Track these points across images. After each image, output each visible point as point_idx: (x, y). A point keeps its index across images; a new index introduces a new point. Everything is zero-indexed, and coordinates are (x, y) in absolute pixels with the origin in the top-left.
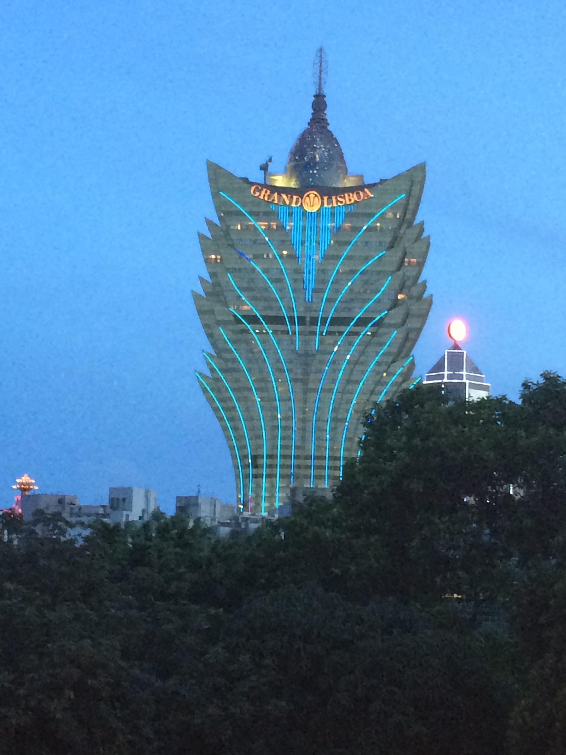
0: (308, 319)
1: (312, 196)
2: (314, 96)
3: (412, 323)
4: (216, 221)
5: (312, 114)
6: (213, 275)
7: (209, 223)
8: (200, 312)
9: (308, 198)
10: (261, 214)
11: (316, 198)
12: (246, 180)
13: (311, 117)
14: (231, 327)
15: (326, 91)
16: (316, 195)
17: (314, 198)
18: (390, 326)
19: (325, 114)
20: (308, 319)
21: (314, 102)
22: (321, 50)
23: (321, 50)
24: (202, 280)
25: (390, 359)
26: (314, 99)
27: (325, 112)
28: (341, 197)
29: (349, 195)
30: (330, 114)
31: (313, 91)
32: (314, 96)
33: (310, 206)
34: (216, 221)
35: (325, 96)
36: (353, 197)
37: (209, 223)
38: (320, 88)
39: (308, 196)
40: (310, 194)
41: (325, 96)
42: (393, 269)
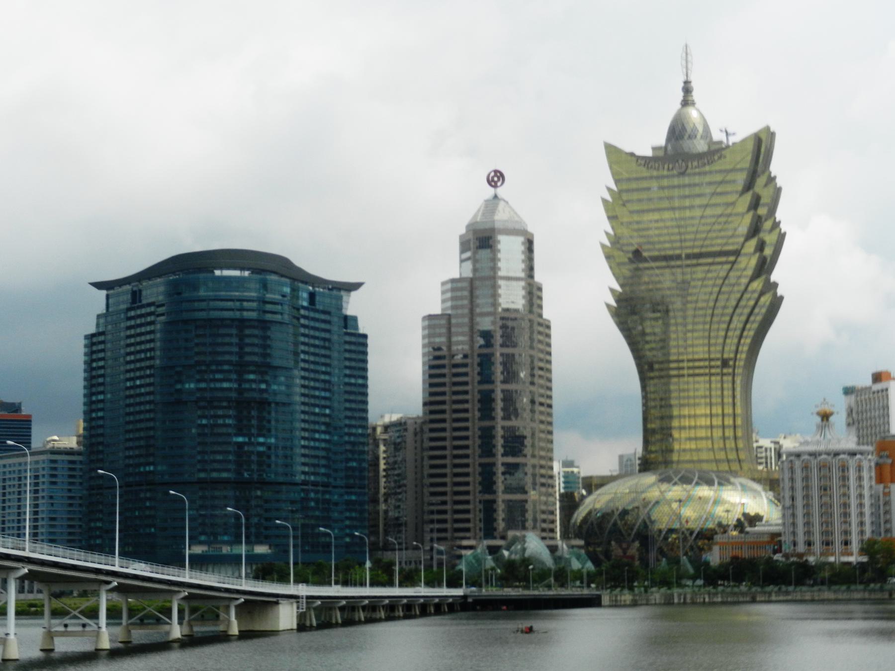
0: (683, 256)
1: (680, 162)
3: (768, 251)
4: (614, 187)
6: (613, 228)
7: (609, 189)
8: (608, 257)
12: (632, 154)
15: (692, 78)
16: (683, 160)
18: (746, 255)
20: (683, 256)
24: (607, 234)
30: (696, 95)
34: (614, 187)
35: (690, 82)
37: (609, 189)
39: (677, 161)
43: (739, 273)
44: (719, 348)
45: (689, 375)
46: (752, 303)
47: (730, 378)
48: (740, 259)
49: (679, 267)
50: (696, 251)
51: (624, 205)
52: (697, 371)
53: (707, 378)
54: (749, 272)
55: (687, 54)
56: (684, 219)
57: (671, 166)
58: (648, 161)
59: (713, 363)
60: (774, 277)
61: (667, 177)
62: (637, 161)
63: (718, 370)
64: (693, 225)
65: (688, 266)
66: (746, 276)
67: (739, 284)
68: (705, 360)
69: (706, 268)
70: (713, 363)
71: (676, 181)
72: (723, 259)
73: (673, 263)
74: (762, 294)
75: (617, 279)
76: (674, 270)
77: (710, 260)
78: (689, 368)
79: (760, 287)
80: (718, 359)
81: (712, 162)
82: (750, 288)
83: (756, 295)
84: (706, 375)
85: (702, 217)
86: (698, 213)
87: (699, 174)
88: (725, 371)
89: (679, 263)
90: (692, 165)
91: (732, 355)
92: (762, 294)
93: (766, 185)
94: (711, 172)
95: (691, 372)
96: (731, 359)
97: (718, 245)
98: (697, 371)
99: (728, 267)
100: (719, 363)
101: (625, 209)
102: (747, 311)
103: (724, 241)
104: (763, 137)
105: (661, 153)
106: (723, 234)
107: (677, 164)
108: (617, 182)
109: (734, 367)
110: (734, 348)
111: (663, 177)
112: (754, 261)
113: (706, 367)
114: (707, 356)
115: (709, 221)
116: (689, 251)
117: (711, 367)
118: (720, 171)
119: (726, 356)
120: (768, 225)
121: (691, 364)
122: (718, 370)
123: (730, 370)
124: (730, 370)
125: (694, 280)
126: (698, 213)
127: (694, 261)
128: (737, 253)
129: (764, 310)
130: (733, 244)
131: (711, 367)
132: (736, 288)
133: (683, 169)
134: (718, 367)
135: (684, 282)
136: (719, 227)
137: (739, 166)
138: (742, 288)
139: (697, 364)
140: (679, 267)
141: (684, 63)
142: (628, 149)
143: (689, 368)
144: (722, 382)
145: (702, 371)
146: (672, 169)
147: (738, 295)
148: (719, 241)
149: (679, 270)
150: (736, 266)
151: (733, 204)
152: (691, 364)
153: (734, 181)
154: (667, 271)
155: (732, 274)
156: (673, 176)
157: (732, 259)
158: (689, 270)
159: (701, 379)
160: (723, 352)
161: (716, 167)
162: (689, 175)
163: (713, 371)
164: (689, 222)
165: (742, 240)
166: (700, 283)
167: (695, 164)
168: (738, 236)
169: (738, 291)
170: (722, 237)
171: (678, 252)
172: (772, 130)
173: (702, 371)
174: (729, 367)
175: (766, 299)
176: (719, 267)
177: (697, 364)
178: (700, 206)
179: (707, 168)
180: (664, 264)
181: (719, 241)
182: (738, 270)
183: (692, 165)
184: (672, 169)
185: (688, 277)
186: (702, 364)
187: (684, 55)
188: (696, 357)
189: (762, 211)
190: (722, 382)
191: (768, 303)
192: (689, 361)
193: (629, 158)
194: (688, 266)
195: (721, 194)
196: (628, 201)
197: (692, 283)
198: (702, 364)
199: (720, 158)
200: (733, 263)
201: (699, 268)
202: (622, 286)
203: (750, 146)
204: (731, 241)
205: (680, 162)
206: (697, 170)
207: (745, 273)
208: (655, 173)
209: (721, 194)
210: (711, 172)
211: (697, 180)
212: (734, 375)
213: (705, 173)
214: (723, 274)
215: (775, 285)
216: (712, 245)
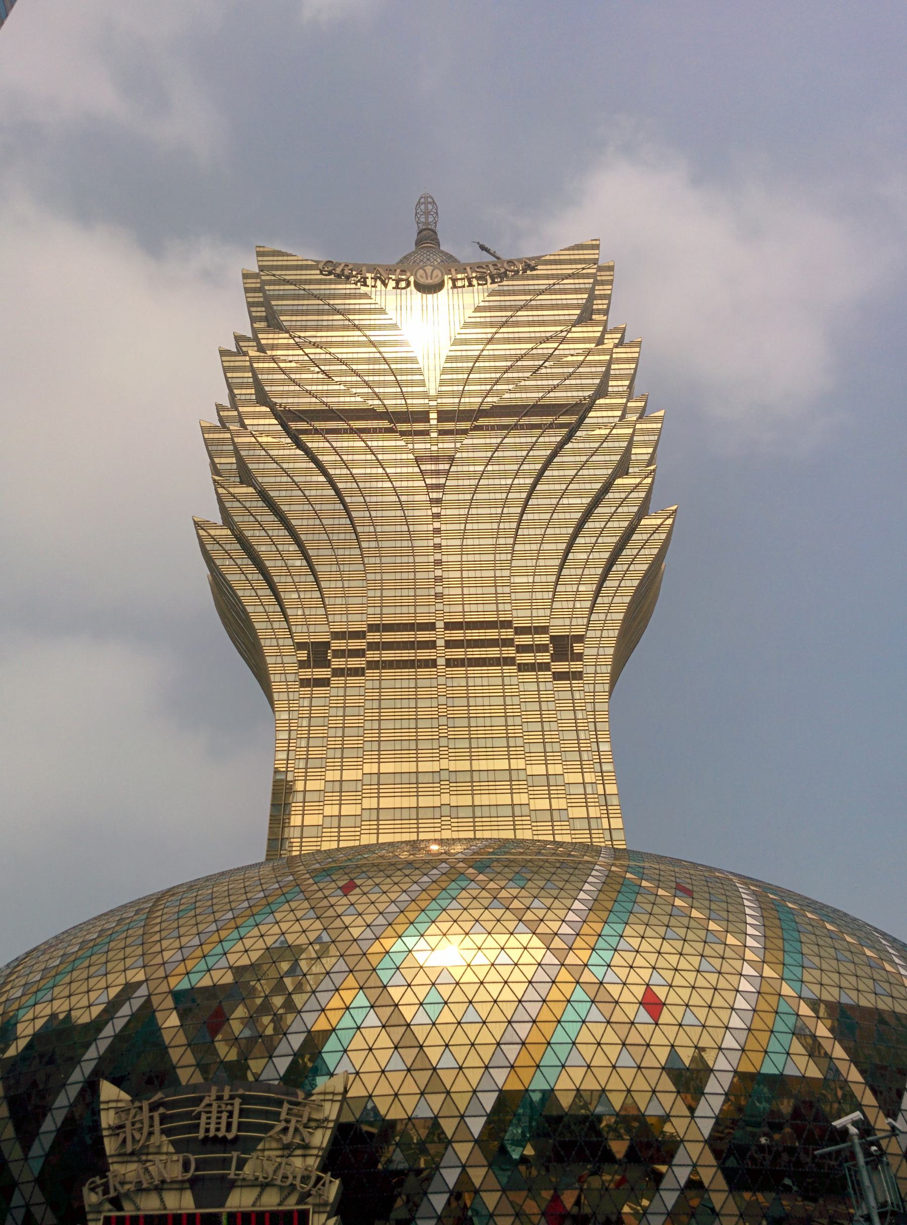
0: (433, 415)
20: (433, 415)
33: (427, 279)
59: (524, 640)
63: (544, 657)
72: (548, 420)
78: (449, 644)
88: (561, 667)
121: (458, 635)
122: (544, 657)
124: (576, 666)
128: (582, 410)
133: (437, 280)
143: (449, 644)
145: (493, 652)
152: (458, 635)
173: (493, 652)
200: (572, 430)
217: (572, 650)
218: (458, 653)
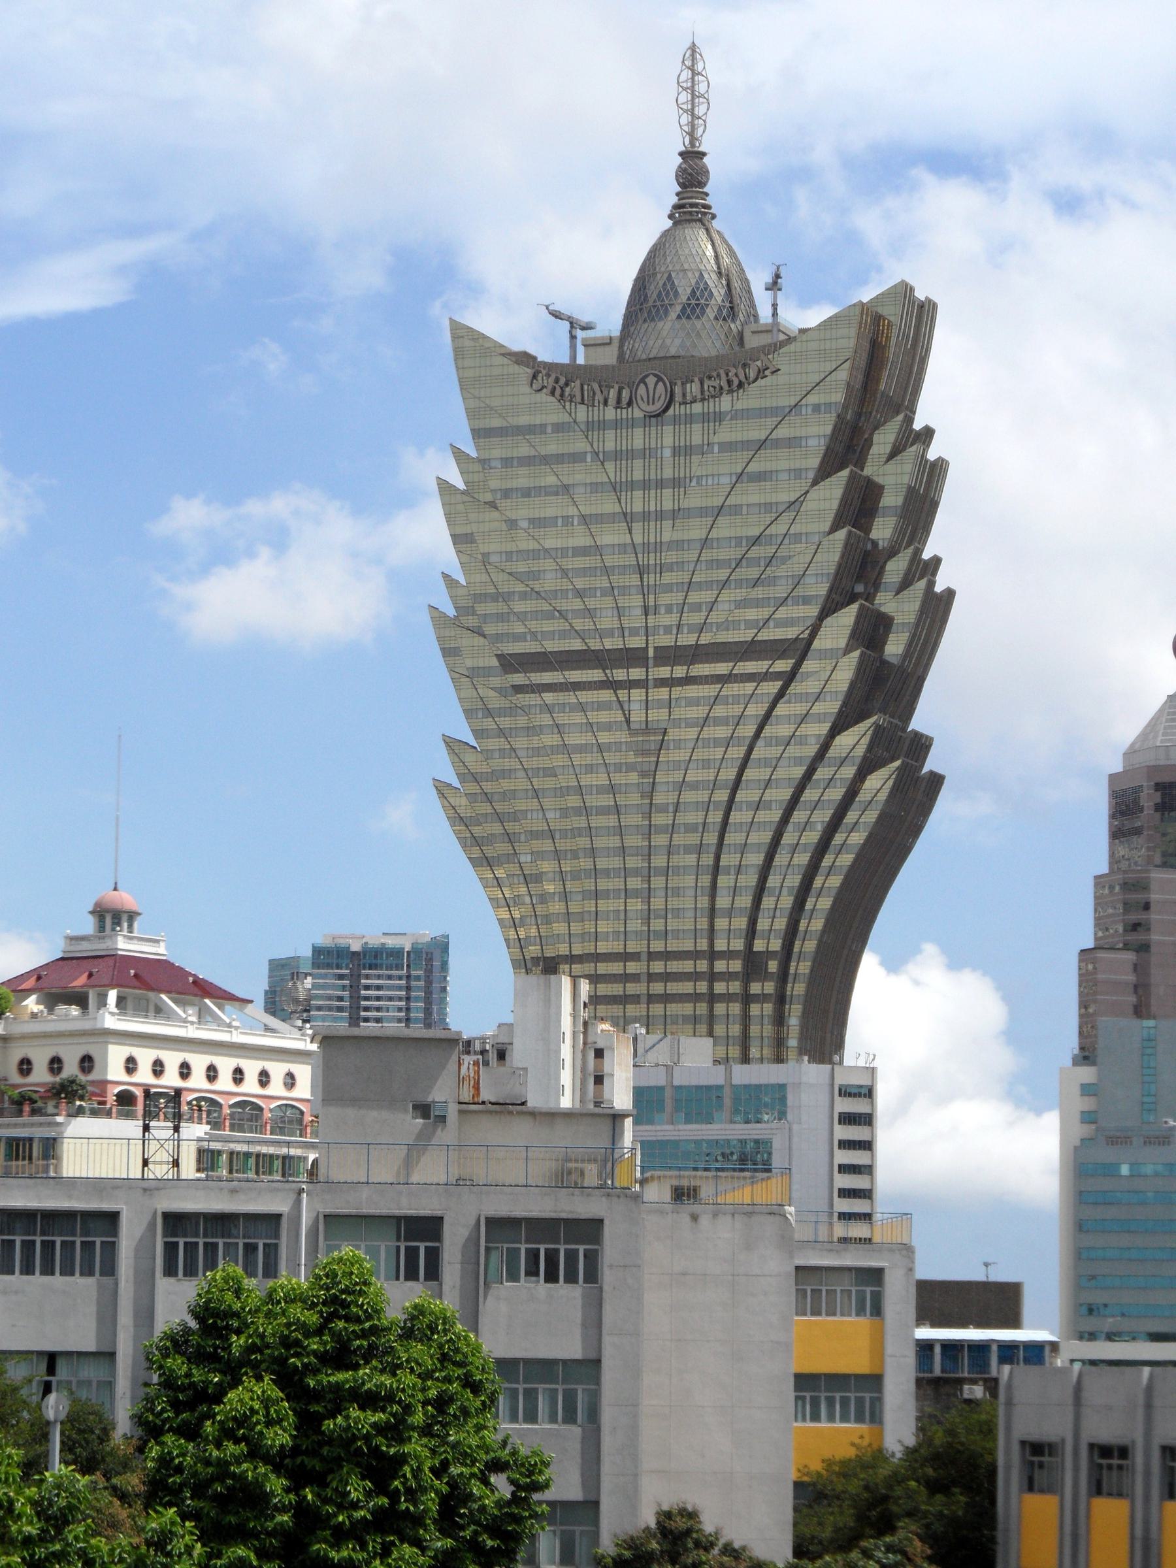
0: (651, 653)
1: (651, 381)
2: (681, 154)
3: (894, 647)
5: (677, 194)
8: (449, 652)
9: (642, 385)
10: (549, 429)
11: (661, 384)
12: (524, 358)
13: (674, 200)
14: (496, 681)
16: (660, 379)
17: (656, 384)
18: (824, 654)
19: (707, 194)
20: (651, 653)
21: (680, 167)
22: (693, 48)
23: (693, 48)
25: (825, 728)
26: (680, 160)
27: (705, 190)
28: (710, 378)
29: (727, 375)
30: (717, 192)
31: (679, 143)
32: (681, 154)
33: (648, 404)
35: (704, 154)
36: (736, 375)
38: (692, 134)
39: (643, 381)
40: (647, 376)
41: (704, 154)
42: (827, 529)
43: (800, 708)
44: (741, 923)
45: (651, 999)
46: (836, 794)
47: (768, 1008)
48: (808, 666)
49: (632, 684)
50: (688, 639)
51: (493, 505)
52: (674, 988)
53: (702, 1008)
54: (831, 707)
55: (695, 73)
56: (659, 547)
57: (625, 394)
58: (562, 380)
59: (720, 966)
60: (918, 723)
61: (616, 424)
62: (534, 377)
63: (735, 987)
64: (680, 565)
65: (662, 683)
66: (820, 718)
67: (803, 741)
68: (695, 955)
69: (711, 690)
70: (720, 966)
71: (638, 439)
73: (620, 674)
74: (866, 768)
75: (469, 713)
76: (622, 694)
77: (722, 668)
78: (651, 977)
79: (860, 751)
80: (729, 955)
81: (741, 385)
82: (831, 753)
83: (849, 772)
84: (695, 998)
85: (705, 542)
86: (695, 530)
87: (705, 418)
88: (755, 988)
89: (636, 673)
90: (684, 395)
91: (776, 945)
92: (866, 768)
93: (893, 455)
94: (736, 415)
95: (658, 988)
96: (769, 954)
97: (749, 624)
98: (674, 988)
99: (773, 687)
100: (736, 966)
101: (495, 515)
102: (823, 816)
103: (765, 613)
104: (891, 312)
105: (608, 357)
106: (759, 592)
107: (642, 390)
108: (479, 434)
109: (783, 976)
110: (781, 924)
111: (602, 425)
112: (845, 673)
113: (695, 976)
114: (703, 945)
115: (723, 554)
116: (665, 640)
117: (712, 977)
118: (763, 413)
119: (759, 945)
120: (895, 568)
121: (658, 967)
123: (770, 987)
125: (677, 723)
126: (695, 530)
127: (680, 671)
128: (801, 649)
129: (871, 816)
130: (789, 622)
131: (712, 977)
132: (792, 751)
133: (658, 406)
134: (729, 976)
135: (647, 728)
136: (754, 573)
137: (812, 399)
138: (811, 750)
139: (675, 966)
140: (632, 684)
141: (684, 97)
142: (516, 348)
143: (651, 977)
144: (746, 1019)
145: (687, 987)
146: (630, 404)
147: (799, 772)
148: (751, 614)
149: (637, 694)
150: (795, 688)
151: (794, 505)
152: (658, 967)
153: (792, 443)
154: (606, 695)
155: (781, 709)
156: (632, 423)
157: (784, 665)
158: (663, 693)
159: (687, 1009)
160: (751, 933)
161: (749, 399)
162: (676, 421)
163: (720, 987)
164: (670, 557)
165: (813, 611)
166: (692, 733)
167: (694, 388)
168: (806, 600)
169: (798, 761)
170: (758, 603)
171: (636, 642)
172: (920, 295)
173: (687, 987)
174: (765, 976)
175: (879, 783)
176: (749, 687)
177: (675, 966)
178: (703, 512)
179: (726, 403)
180: (596, 675)
181: (751, 614)
182: (801, 698)
183: (684, 395)
184: (630, 404)
185: (659, 715)
186: (687, 966)
187: (687, 74)
188: (673, 946)
189: (882, 531)
190: (746, 1019)
191: (883, 796)
192: (652, 956)
193: (516, 369)
194: (662, 683)
195: (761, 477)
196: (507, 493)
197: (672, 734)
198: (687, 966)
199: (761, 374)
200: (790, 678)
201: (692, 691)
202: (478, 733)
203: (848, 341)
204: (782, 613)
205: (651, 381)
206: (697, 408)
207: (818, 708)
208: (582, 413)
209: (761, 477)
210: (736, 415)
211: (696, 436)
212: (781, 999)
213: (719, 417)
214: (756, 710)
215: (921, 745)
216: (727, 625)
217: (766, 968)
218: (658, 988)
